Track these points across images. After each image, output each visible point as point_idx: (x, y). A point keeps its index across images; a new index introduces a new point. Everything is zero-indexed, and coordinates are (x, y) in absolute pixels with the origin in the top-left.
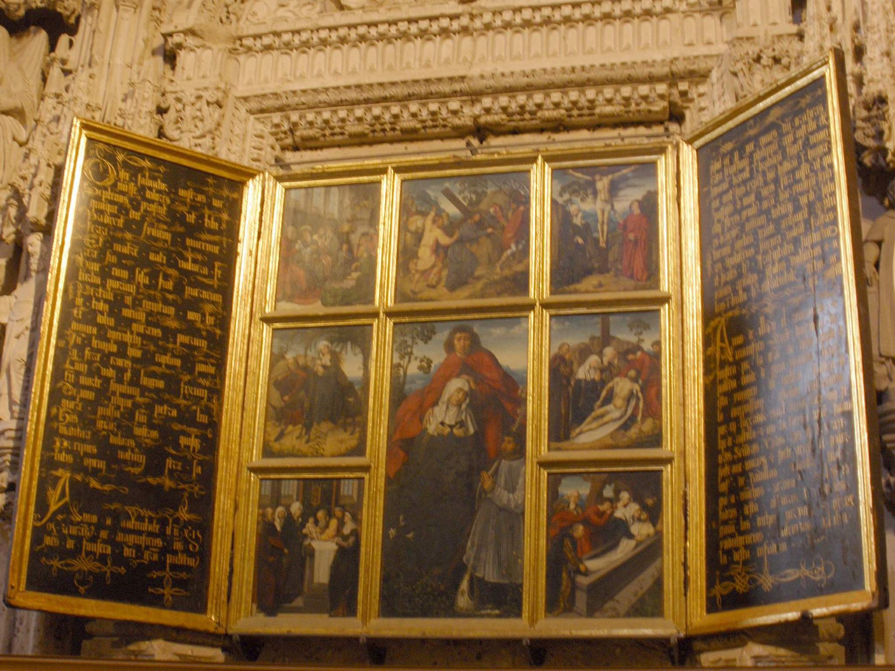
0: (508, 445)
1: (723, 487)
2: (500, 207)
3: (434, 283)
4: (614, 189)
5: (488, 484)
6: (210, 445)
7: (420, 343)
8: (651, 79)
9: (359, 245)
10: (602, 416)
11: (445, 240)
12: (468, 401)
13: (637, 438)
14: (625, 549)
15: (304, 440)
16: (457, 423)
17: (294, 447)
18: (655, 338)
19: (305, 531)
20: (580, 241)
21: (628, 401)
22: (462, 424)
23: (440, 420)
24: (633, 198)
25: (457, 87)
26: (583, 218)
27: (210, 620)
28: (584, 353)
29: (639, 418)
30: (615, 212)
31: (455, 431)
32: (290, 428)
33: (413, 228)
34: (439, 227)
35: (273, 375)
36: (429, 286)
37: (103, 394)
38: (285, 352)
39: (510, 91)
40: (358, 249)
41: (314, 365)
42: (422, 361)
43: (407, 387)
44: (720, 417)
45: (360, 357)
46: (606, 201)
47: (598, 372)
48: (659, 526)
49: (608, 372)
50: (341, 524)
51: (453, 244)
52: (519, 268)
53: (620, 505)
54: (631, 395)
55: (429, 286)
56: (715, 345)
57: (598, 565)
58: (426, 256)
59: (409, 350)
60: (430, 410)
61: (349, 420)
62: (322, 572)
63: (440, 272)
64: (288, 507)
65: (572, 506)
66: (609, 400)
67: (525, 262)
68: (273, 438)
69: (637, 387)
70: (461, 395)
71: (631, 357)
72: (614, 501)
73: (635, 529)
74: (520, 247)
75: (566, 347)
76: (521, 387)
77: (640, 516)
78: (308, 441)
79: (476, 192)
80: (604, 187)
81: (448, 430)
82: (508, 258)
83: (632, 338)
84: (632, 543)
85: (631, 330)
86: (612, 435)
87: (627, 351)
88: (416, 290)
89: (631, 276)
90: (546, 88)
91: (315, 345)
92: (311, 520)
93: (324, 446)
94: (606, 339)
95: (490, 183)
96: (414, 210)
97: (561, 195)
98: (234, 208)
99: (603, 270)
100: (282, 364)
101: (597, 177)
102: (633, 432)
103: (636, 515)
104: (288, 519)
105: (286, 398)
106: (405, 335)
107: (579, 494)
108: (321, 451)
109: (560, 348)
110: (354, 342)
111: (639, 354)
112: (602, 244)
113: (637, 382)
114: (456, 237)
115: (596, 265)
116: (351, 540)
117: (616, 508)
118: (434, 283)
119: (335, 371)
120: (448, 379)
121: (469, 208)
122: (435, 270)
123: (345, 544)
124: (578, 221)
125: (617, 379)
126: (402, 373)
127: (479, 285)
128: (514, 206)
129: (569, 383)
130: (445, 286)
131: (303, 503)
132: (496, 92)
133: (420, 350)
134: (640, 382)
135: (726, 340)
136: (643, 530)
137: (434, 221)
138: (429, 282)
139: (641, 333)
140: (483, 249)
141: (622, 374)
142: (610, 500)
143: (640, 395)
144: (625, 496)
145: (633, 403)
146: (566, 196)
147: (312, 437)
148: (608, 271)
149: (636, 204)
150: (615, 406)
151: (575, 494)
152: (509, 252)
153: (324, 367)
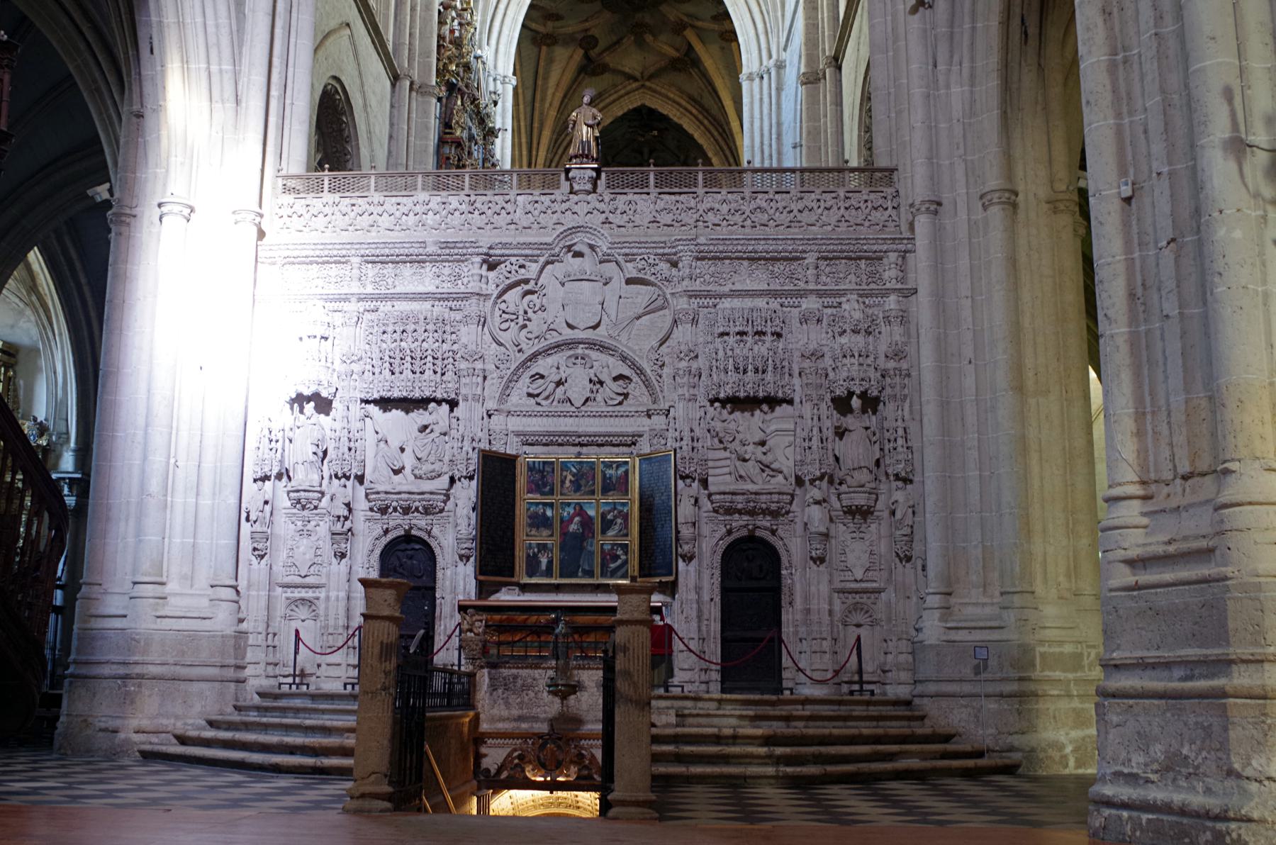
4: (617, 467)
8: (628, 436)
14: (619, 562)
27: (515, 580)
39: (590, 436)
49: (615, 517)
57: (613, 566)
58: (568, 484)
62: (544, 567)
87: (620, 512)
90: (599, 436)
94: (615, 509)
98: (514, 468)
104: (534, 553)
119: (544, 513)
132: (585, 436)
133: (567, 509)
136: (623, 557)
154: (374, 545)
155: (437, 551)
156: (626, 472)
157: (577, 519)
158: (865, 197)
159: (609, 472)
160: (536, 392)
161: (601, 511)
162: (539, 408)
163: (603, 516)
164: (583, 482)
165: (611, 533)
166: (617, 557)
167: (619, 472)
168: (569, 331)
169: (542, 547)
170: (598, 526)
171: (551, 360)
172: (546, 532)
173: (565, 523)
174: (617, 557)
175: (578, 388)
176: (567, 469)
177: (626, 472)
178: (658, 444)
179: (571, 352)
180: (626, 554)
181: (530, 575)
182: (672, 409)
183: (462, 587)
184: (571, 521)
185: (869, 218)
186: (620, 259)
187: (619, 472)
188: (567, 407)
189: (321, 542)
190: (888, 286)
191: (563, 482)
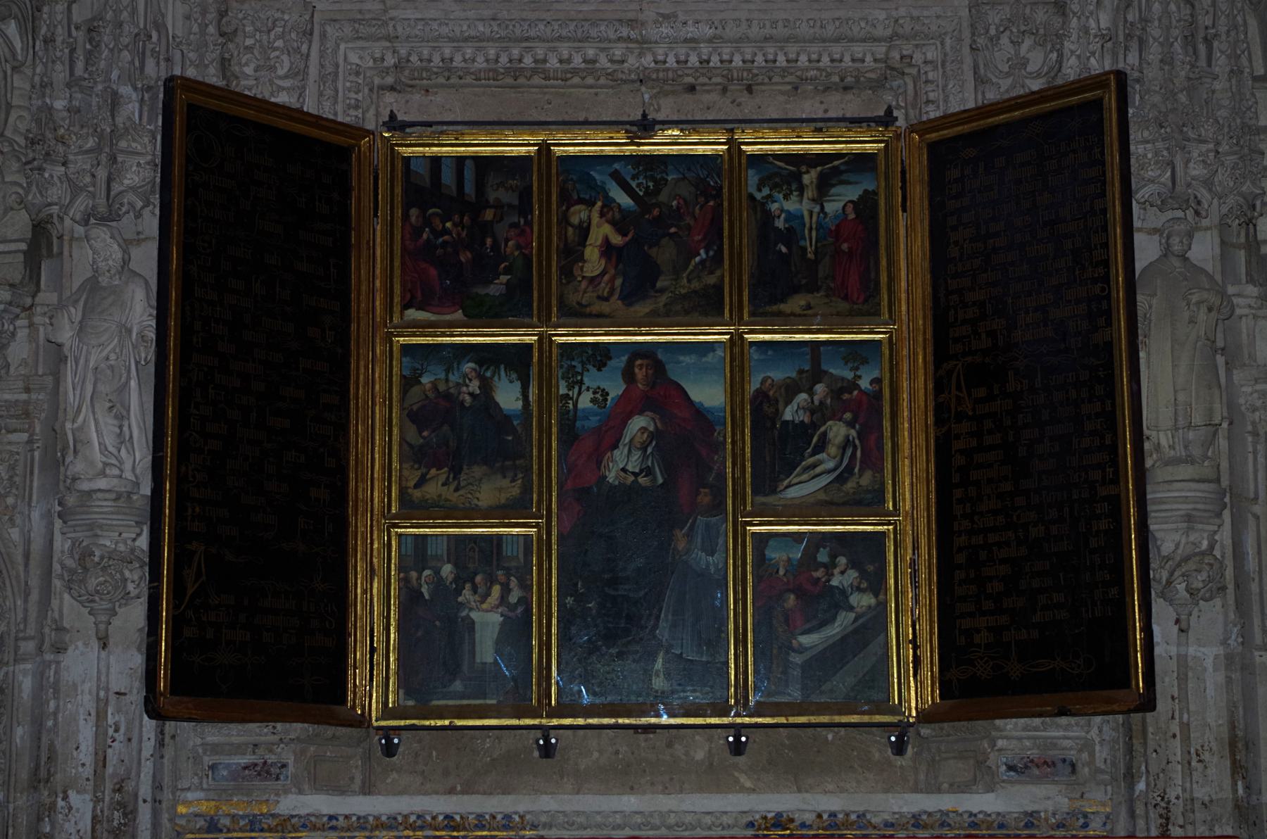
0: (705, 498)
1: (960, 559)
2: (685, 201)
3: (605, 294)
4: (824, 186)
5: (681, 545)
7: (593, 370)
9: (507, 240)
10: (814, 466)
11: (617, 240)
12: (654, 443)
13: (854, 493)
14: (842, 623)
15: (452, 487)
16: (641, 471)
17: (440, 496)
18: (876, 374)
19: (460, 599)
20: (784, 249)
21: (843, 448)
22: (648, 472)
23: (621, 466)
24: (848, 199)
25: (625, 32)
26: (786, 220)
28: (791, 389)
29: (856, 470)
30: (826, 214)
31: (641, 480)
32: (433, 471)
33: (575, 220)
34: (608, 222)
35: (406, 405)
36: (599, 297)
38: (421, 375)
40: (506, 245)
41: (459, 393)
42: (595, 393)
43: (578, 424)
44: (956, 479)
45: (518, 385)
46: (813, 200)
47: (808, 413)
48: (881, 597)
49: (820, 413)
50: (506, 590)
51: (626, 244)
52: (711, 280)
53: (836, 571)
54: (847, 442)
55: (599, 297)
56: (950, 393)
58: (593, 261)
59: (579, 378)
60: (609, 454)
61: (508, 463)
63: (612, 280)
64: (437, 572)
65: (781, 572)
66: (821, 447)
67: (718, 273)
68: (412, 484)
69: (853, 433)
70: (645, 435)
71: (846, 396)
72: (829, 567)
73: (854, 599)
74: (711, 253)
75: (769, 381)
76: (718, 428)
77: (860, 583)
78: (457, 490)
79: (653, 178)
80: (812, 182)
81: (632, 478)
82: (697, 265)
83: (849, 375)
84: (852, 615)
85: (846, 363)
86: (825, 488)
87: (841, 389)
88: (584, 302)
89: (846, 298)
91: (458, 368)
92: (468, 586)
93: (478, 495)
94: (817, 375)
95: (670, 167)
96: (576, 197)
97: (760, 190)
99: (812, 288)
100: (416, 389)
101: (804, 169)
102: (850, 485)
103: (855, 584)
104: (438, 582)
105: (425, 434)
106: (573, 359)
107: (789, 560)
108: (475, 501)
109: (764, 381)
110: (510, 367)
111: (856, 393)
112: (810, 256)
113: (854, 427)
114: (630, 237)
115: (804, 282)
116: (520, 610)
117: (833, 575)
118: (605, 294)
120: (630, 416)
121: (646, 199)
122: (606, 278)
123: (511, 614)
124: (780, 223)
125: (830, 423)
126: (571, 406)
127: (663, 299)
128: (702, 200)
129: (774, 424)
130: (619, 299)
131: (456, 565)
133: (592, 379)
134: (857, 427)
135: (964, 389)
136: (862, 601)
137: (602, 215)
138: (600, 293)
139: (857, 369)
140: (664, 254)
141: (835, 416)
142: (824, 565)
143: (857, 442)
144: (842, 561)
145: (849, 452)
146: (766, 191)
147: (462, 484)
148: (818, 290)
149: (850, 208)
150: (829, 455)
151: (785, 558)
152: (697, 259)
153: (471, 394)
157: (638, 423)
159: (787, 206)
161: (754, 385)
164: (664, 254)
165: (800, 489)
167: (832, 207)
172: (489, 491)
176: (593, 194)
183: (86, 754)
184: (609, 435)
187: (832, 207)
191: (572, 254)
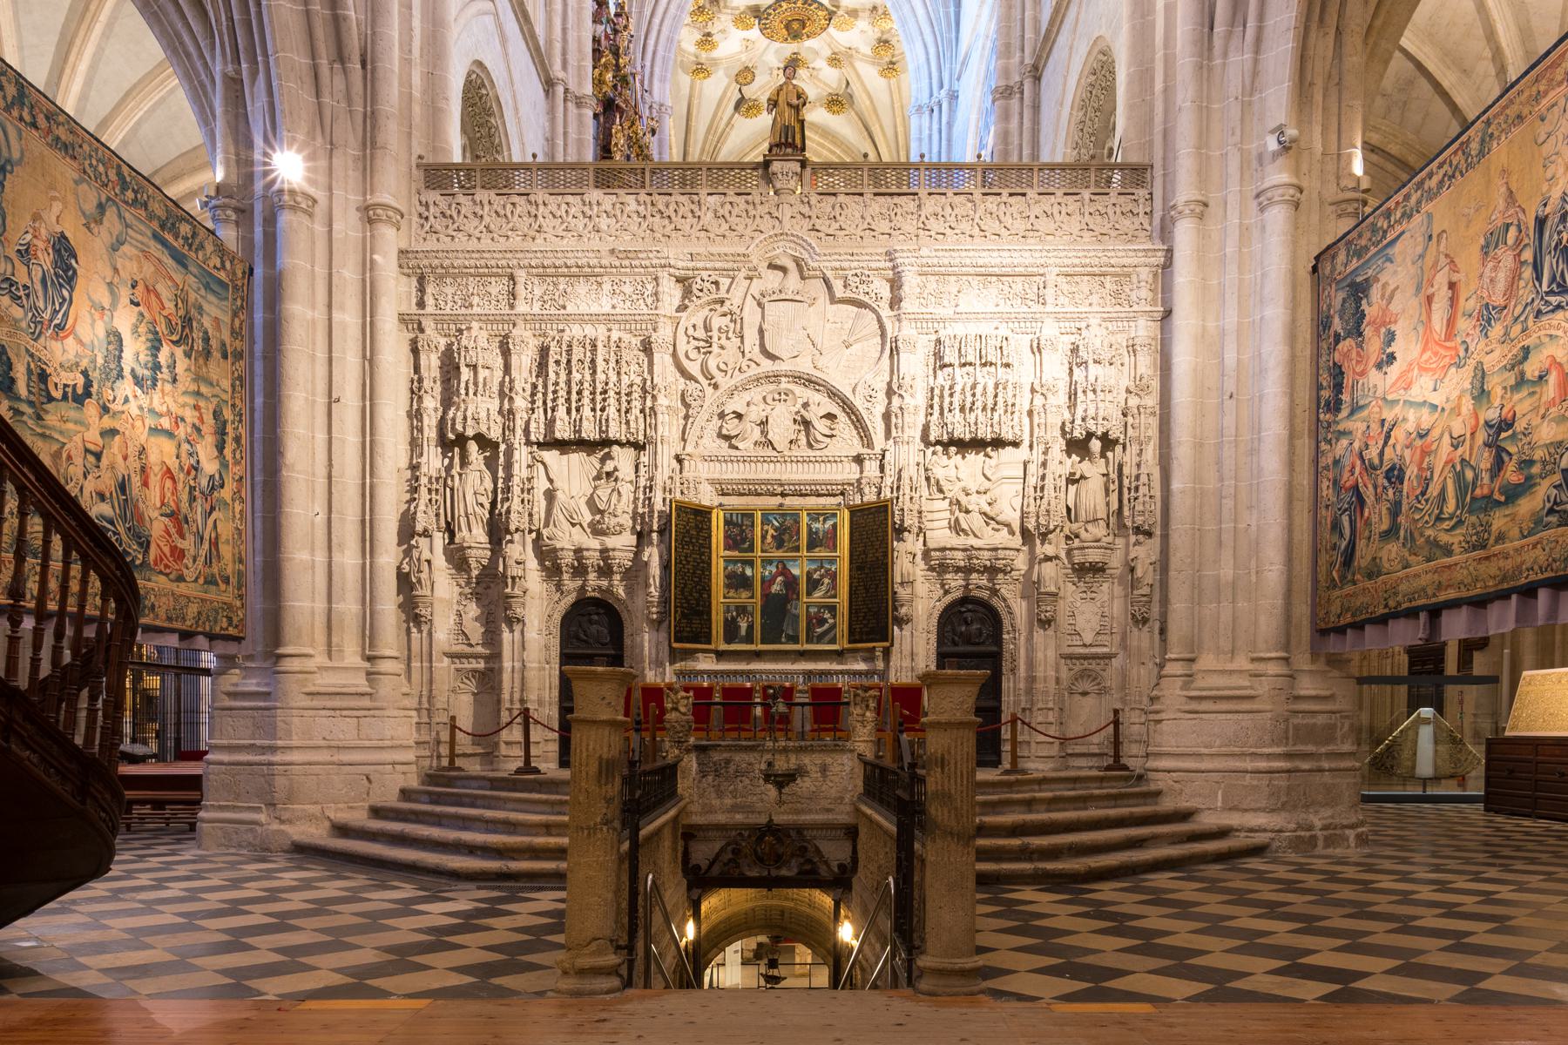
4: (825, 520)
6: (710, 596)
14: (827, 626)
27: (712, 647)
28: (816, 571)
37: (685, 584)
49: (822, 576)
58: (769, 537)
62: (743, 632)
87: (827, 571)
94: (822, 567)
98: (710, 520)
119: (743, 573)
133: (769, 568)
136: (831, 621)
140: (786, 537)
154: (553, 609)
155: (624, 616)
156: (835, 526)
158: (1114, 200)
159: (816, 526)
160: (733, 433)
162: (737, 453)
163: (809, 574)
164: (786, 537)
165: (818, 595)
166: (822, 621)
168: (769, 362)
169: (742, 610)
170: (803, 586)
171: (746, 396)
172: (745, 594)
173: (767, 583)
174: (822, 621)
175: (782, 429)
177: (835, 526)
178: (870, 496)
179: (772, 387)
180: (834, 617)
181: (728, 640)
182: (887, 454)
184: (772, 581)
185: (1117, 226)
186: (829, 274)
188: (770, 452)
189: (493, 607)
190: (1136, 308)
